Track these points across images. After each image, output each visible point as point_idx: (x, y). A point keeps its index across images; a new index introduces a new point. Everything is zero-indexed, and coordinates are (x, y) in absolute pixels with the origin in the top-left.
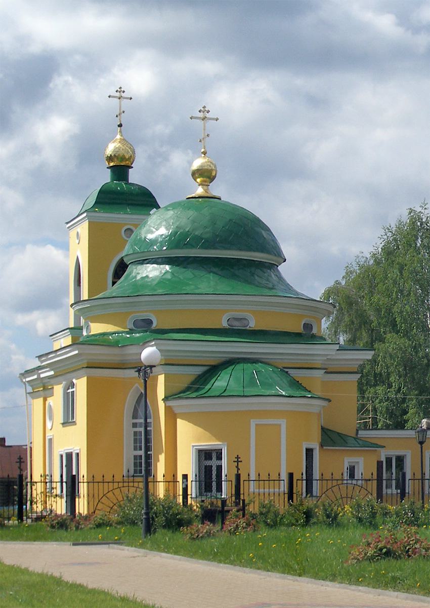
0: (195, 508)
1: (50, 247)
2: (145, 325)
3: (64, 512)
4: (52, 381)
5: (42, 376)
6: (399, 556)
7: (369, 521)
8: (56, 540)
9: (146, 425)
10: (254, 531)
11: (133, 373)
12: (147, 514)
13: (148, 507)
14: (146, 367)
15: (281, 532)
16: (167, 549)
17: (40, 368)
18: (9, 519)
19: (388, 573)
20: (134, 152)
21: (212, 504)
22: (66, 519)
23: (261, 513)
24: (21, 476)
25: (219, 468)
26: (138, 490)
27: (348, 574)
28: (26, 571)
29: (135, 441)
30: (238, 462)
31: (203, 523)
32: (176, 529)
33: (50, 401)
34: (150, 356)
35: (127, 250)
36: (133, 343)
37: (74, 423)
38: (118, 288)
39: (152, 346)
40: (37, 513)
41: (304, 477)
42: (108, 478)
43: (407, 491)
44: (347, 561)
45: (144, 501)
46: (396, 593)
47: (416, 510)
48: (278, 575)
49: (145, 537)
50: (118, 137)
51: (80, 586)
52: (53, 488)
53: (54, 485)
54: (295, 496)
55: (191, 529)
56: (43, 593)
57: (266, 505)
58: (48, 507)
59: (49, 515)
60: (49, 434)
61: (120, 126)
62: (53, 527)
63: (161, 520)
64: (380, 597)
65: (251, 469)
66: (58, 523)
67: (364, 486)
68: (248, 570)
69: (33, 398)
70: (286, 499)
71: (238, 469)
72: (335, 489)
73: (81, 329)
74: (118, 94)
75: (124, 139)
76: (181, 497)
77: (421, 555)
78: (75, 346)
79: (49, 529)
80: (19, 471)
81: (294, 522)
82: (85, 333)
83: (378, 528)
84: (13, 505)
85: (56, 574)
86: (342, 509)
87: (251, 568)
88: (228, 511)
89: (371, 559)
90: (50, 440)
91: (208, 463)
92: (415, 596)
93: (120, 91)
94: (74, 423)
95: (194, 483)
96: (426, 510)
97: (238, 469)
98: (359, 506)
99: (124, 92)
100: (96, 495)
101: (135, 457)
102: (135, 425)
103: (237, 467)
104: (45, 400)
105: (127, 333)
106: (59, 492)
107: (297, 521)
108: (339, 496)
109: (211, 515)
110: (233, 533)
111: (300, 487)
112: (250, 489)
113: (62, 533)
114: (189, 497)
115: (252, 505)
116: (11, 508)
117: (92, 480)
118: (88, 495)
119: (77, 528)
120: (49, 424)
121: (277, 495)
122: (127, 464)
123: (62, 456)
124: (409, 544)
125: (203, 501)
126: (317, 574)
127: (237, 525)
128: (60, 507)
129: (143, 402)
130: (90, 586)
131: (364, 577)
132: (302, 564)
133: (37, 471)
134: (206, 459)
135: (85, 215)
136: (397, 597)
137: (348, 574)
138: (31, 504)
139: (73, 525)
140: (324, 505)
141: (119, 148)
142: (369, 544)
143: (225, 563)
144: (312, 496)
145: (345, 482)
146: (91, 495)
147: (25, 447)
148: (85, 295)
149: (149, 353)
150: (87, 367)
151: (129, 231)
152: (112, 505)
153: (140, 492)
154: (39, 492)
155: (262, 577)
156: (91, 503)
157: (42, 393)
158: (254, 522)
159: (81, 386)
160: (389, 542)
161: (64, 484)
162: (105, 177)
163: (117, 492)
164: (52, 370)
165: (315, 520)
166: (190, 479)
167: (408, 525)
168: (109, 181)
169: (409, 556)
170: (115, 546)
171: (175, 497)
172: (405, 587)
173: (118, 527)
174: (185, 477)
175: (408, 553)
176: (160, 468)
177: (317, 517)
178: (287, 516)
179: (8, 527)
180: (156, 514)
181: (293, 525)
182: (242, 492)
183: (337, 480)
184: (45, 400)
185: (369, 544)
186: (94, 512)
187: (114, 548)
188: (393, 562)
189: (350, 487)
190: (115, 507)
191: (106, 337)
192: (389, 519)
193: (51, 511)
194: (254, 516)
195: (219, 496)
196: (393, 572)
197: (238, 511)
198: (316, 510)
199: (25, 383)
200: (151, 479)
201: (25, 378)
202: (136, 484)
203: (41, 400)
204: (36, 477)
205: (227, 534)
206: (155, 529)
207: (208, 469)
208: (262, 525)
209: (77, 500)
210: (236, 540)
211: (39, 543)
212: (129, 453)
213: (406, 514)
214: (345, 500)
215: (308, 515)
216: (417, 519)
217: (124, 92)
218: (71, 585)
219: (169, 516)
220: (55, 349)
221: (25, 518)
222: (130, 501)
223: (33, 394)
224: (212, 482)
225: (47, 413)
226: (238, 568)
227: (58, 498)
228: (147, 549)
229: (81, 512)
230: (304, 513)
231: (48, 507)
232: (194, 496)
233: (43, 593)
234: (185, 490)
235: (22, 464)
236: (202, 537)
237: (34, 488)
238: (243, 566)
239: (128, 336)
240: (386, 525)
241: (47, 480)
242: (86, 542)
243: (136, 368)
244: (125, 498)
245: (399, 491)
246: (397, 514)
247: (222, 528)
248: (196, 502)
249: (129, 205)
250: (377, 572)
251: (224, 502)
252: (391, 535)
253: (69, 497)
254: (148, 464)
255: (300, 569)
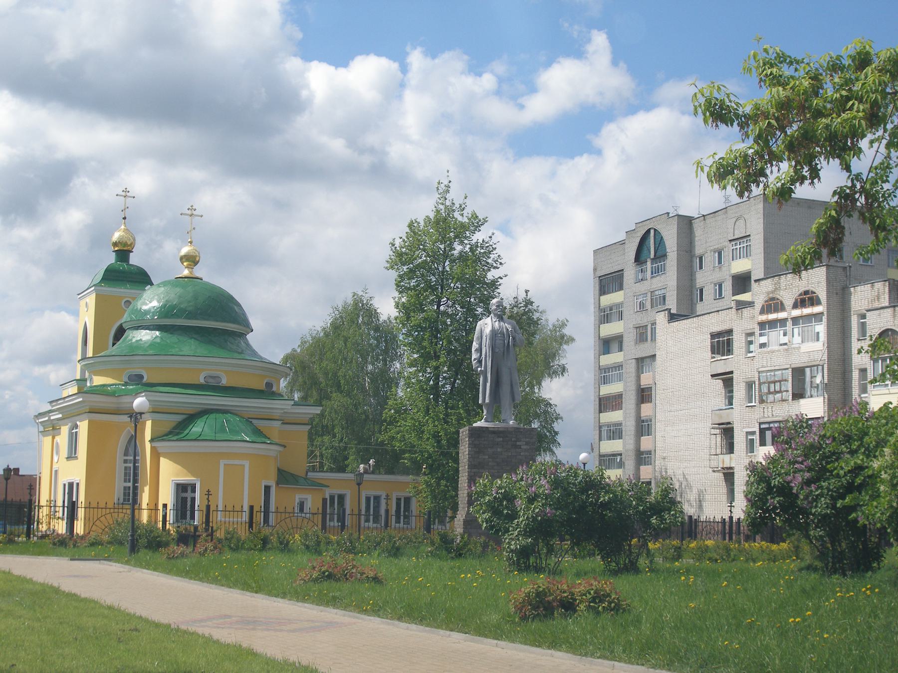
0: (172, 532)
1: (63, 313)
2: (137, 379)
3: (64, 532)
4: (60, 422)
5: (52, 418)
6: (339, 579)
7: (315, 548)
8: (57, 556)
9: (135, 461)
10: (220, 553)
11: (126, 418)
12: (132, 536)
13: (134, 529)
14: (137, 413)
15: (242, 556)
16: (147, 566)
17: (50, 411)
18: (19, 536)
19: (329, 593)
20: (134, 239)
21: (186, 529)
22: (66, 538)
23: (226, 539)
24: (31, 501)
25: (193, 499)
26: (126, 515)
27: (296, 592)
28: (30, 581)
29: (125, 474)
30: (209, 495)
31: (178, 545)
32: (156, 550)
33: (58, 439)
34: (140, 404)
35: (126, 317)
36: (127, 393)
37: (76, 458)
38: (117, 348)
39: (142, 396)
40: (42, 532)
41: (263, 510)
42: (102, 505)
43: (346, 524)
44: (295, 581)
45: (130, 525)
46: (335, 611)
47: (353, 540)
48: (239, 591)
49: (130, 555)
50: (123, 227)
51: (75, 595)
52: (56, 512)
53: (57, 509)
54: (254, 525)
55: (168, 550)
56: (44, 600)
57: (231, 532)
58: (52, 527)
59: (52, 534)
60: (55, 467)
61: (125, 218)
62: (54, 544)
63: (143, 541)
64: (322, 613)
65: (219, 501)
66: (59, 541)
67: (311, 519)
68: (213, 586)
69: (44, 436)
70: (247, 528)
71: (209, 501)
72: (288, 520)
73: (86, 380)
74: (124, 194)
75: (127, 229)
76: (161, 523)
77: (357, 578)
78: (80, 395)
79: (51, 545)
80: (29, 496)
81: (253, 547)
82: (88, 384)
83: (322, 554)
84: (23, 524)
85: (56, 585)
86: (293, 538)
87: (216, 584)
88: (199, 536)
89: (316, 580)
90: (56, 471)
91: (184, 495)
92: (351, 613)
93: (126, 191)
94: (76, 458)
95: (172, 511)
96: (361, 540)
97: (209, 501)
98: (307, 535)
99: (129, 192)
100: (91, 519)
101: (125, 488)
102: (125, 461)
103: (208, 499)
104: (53, 438)
105: (123, 385)
106: (61, 515)
107: (256, 546)
108: (290, 526)
109: (186, 538)
110: (202, 554)
111: (259, 518)
112: (218, 518)
113: (62, 549)
114: (168, 523)
115: (218, 532)
116: (21, 527)
117: (88, 506)
118: (85, 519)
119: (74, 546)
120: (55, 458)
121: (239, 523)
122: (118, 493)
123: (65, 485)
124: (347, 569)
125: (179, 527)
126: (271, 592)
127: (206, 548)
128: (61, 527)
129: (133, 444)
130: (83, 596)
131: (309, 595)
132: (258, 583)
133: (44, 497)
134: (182, 492)
135: (93, 288)
136: (336, 614)
137: (296, 592)
138: (38, 525)
139: (71, 543)
140: (278, 534)
141: (123, 236)
142: (314, 568)
143: (195, 580)
144: (268, 525)
145: (296, 515)
146: (87, 518)
147: (35, 477)
148: (90, 353)
149: (140, 402)
150: (89, 412)
151: (128, 303)
152: (104, 527)
153: (127, 518)
154: (45, 514)
155: (226, 593)
156: (87, 525)
157: (51, 432)
158: (220, 546)
159: (83, 427)
160: (330, 566)
161: (66, 509)
162: (110, 259)
163: (109, 516)
164: (61, 413)
165: (270, 546)
166: (169, 507)
167: (347, 553)
168: (114, 261)
169: (347, 579)
170: (105, 562)
171: (156, 522)
172: (343, 606)
173: (108, 546)
174: (165, 506)
175: (346, 576)
176: (145, 498)
177: (272, 543)
178: (247, 542)
179: (17, 543)
180: (139, 536)
181: (252, 549)
182: (211, 520)
183: (290, 513)
184: (53, 438)
185: (314, 568)
186: (89, 533)
187: (104, 564)
188: (334, 584)
189: (300, 519)
190: (107, 529)
191: (105, 388)
192: (331, 547)
193: (54, 531)
194: (220, 541)
195: (192, 523)
196: (333, 592)
197: (207, 536)
198: (272, 538)
199: (37, 423)
200: (136, 507)
201: (38, 419)
202: (124, 511)
203: (50, 437)
204: (43, 502)
205: (198, 555)
206: (139, 549)
207: (184, 500)
208: (226, 549)
209: (75, 522)
210: (204, 561)
211: (43, 557)
212: (119, 485)
213: (345, 543)
214: (295, 530)
215: (265, 541)
216: (354, 548)
217: (129, 192)
218: (68, 594)
219: (150, 539)
220: (63, 397)
221: (32, 536)
222: (119, 525)
223: (44, 433)
224: (187, 511)
225: (55, 448)
226: (205, 584)
227: (60, 520)
228: (131, 565)
229: (79, 532)
230: (261, 540)
231: (51, 527)
232: (171, 522)
233: (44, 600)
234: (165, 517)
235: (32, 490)
236: (177, 557)
237: (41, 510)
238: (210, 583)
239: (123, 388)
240: (328, 552)
241: (52, 504)
242: (81, 557)
243: (128, 414)
244: (115, 522)
245: (340, 524)
246: (338, 543)
247: (194, 550)
248: (173, 528)
249: (129, 281)
250: (320, 591)
251: (196, 528)
252: (333, 561)
253: (69, 520)
254: (135, 494)
255: (257, 587)
